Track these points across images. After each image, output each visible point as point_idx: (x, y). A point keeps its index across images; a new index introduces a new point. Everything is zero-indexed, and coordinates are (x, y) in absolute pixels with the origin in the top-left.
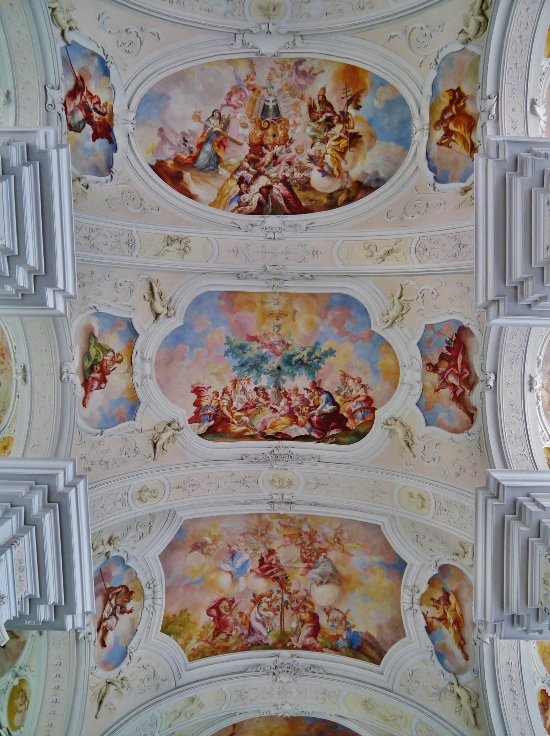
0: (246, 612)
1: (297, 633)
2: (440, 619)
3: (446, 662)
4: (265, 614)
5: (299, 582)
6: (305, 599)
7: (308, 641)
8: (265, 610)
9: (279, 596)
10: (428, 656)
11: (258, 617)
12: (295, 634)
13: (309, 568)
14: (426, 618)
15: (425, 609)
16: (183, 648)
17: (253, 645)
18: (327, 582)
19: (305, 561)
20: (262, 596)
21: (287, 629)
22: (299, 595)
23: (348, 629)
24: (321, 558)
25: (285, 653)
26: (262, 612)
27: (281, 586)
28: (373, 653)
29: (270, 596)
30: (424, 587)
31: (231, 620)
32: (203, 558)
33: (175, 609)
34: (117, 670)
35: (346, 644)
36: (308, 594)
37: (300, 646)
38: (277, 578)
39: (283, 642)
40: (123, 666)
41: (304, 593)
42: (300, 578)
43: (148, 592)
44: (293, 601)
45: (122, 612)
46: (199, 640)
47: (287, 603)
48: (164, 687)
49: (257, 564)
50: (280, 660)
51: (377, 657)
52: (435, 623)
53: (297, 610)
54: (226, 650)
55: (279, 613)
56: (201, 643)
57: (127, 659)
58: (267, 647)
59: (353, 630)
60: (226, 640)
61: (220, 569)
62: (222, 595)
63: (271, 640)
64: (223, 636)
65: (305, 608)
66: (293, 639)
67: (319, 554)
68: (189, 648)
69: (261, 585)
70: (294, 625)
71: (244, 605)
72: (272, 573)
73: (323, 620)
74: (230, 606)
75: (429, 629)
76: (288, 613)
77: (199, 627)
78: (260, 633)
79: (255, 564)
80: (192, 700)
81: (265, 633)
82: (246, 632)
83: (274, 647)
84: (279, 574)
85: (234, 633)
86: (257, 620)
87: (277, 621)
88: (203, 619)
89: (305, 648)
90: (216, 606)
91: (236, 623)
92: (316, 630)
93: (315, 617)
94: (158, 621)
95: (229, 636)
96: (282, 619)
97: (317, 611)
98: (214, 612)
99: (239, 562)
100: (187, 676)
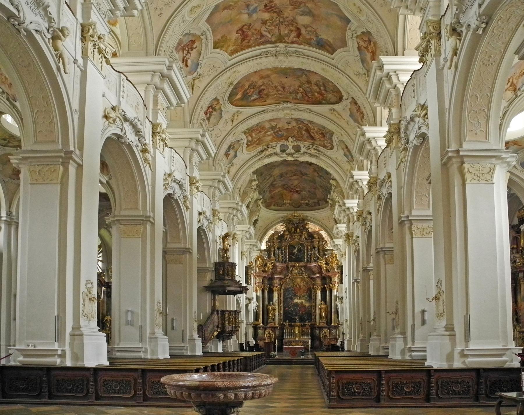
0: (258, 28)
1: (288, 35)
2: (365, 48)
3: (365, 65)
4: (270, 28)
5: (288, 13)
6: (292, 21)
7: (294, 39)
8: (269, 26)
9: (278, 19)
10: (357, 59)
11: (266, 29)
12: (287, 36)
13: (295, 8)
14: (358, 44)
15: (359, 41)
16: (226, 51)
17: (263, 42)
18: (306, 15)
19: (293, 5)
20: (267, 20)
21: (282, 33)
22: (290, 18)
23: (317, 37)
24: (302, 5)
25: (282, 45)
26: (268, 27)
27: (278, 15)
28: (330, 49)
29: (272, 20)
30: (359, 33)
31: (250, 33)
32: (230, 11)
33: (219, 37)
34: (196, 73)
35: (315, 43)
36: (295, 18)
37: (290, 42)
38: (275, 12)
39: (280, 39)
40: (199, 70)
41: (292, 18)
42: (290, 12)
43: (202, 37)
44: (285, 21)
45: (192, 50)
46: (233, 46)
47: (282, 22)
48: (219, 70)
49: (263, 7)
50: (279, 49)
51: (331, 51)
52: (362, 48)
53: (288, 25)
54: (249, 47)
55: (278, 27)
56: (235, 47)
57: (200, 66)
58: (271, 42)
59: (319, 37)
60: (248, 42)
61: (241, 13)
62: (244, 24)
63: (273, 39)
64: (247, 41)
65: (293, 25)
66: (286, 39)
67: (300, 4)
68: (229, 51)
69: (266, 16)
70: (286, 32)
71: (258, 25)
72: (272, 10)
73: (303, 31)
74: (249, 27)
75: (359, 49)
76: (282, 27)
77: (233, 40)
78: (267, 37)
79: (262, 7)
80: (235, 72)
81: (270, 36)
82: (259, 37)
83: (275, 42)
84: (277, 10)
85: (252, 38)
86: (265, 31)
87: (277, 31)
88: (234, 36)
89: (293, 42)
90: (241, 29)
91: (253, 34)
92: (299, 35)
93: (298, 29)
94: (211, 45)
95: (250, 40)
96: (279, 29)
97: (299, 27)
98: (240, 32)
99: (252, 8)
100: (230, 63)
